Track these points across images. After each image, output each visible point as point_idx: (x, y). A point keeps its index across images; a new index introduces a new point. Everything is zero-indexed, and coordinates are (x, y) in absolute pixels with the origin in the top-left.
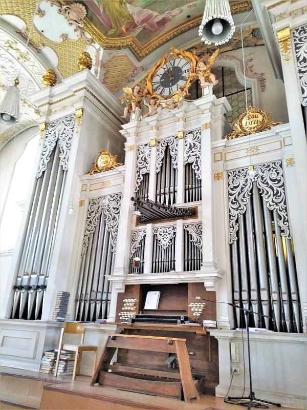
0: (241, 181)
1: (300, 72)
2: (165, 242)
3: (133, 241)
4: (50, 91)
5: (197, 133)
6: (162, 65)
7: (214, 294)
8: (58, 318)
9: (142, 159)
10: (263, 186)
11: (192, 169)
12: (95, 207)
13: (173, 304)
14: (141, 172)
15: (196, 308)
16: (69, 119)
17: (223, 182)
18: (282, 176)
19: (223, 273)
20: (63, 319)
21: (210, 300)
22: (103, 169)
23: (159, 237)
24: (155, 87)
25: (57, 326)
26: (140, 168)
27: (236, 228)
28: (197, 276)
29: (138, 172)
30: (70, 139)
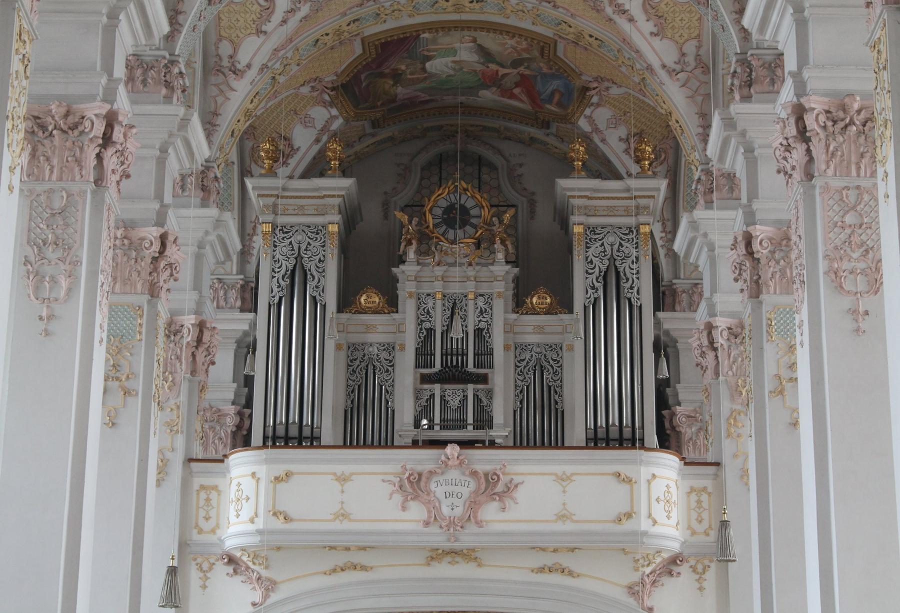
0: (528, 357)
1: (587, 272)
2: (454, 403)
3: (417, 398)
5: (488, 298)
10: (545, 364)
12: (359, 354)
14: (423, 325)
17: (512, 354)
18: (561, 357)
23: (447, 398)
26: (422, 321)
27: (521, 396)
29: (419, 325)
30: (320, 261)
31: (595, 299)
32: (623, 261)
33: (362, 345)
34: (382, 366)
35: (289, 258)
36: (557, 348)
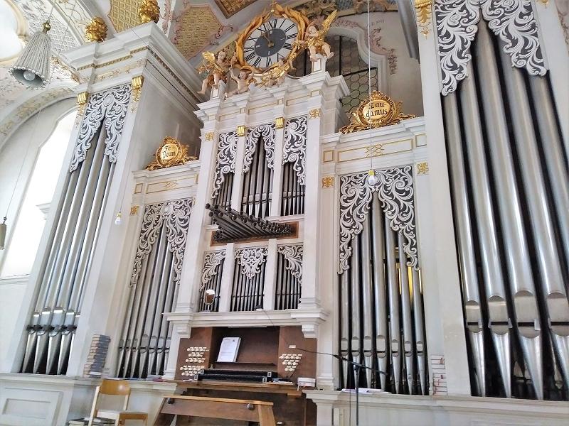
0: (359, 191)
1: (441, 49)
2: (251, 269)
3: (206, 266)
4: (97, 49)
6: (260, 24)
7: (313, 342)
8: (92, 373)
9: (224, 152)
10: (386, 199)
11: (293, 171)
12: (154, 217)
13: (257, 355)
14: (222, 170)
15: (288, 360)
16: (123, 90)
17: (334, 191)
18: (412, 186)
19: (328, 314)
20: (99, 374)
21: (309, 350)
22: (167, 164)
23: (244, 263)
24: (247, 54)
25: (90, 383)
26: (221, 165)
27: (348, 252)
28: (293, 316)
30: (122, 118)
31: (460, 83)
32: (502, 20)
33: (159, 205)
34: (176, 228)
35: (95, 122)
36: (404, 173)
